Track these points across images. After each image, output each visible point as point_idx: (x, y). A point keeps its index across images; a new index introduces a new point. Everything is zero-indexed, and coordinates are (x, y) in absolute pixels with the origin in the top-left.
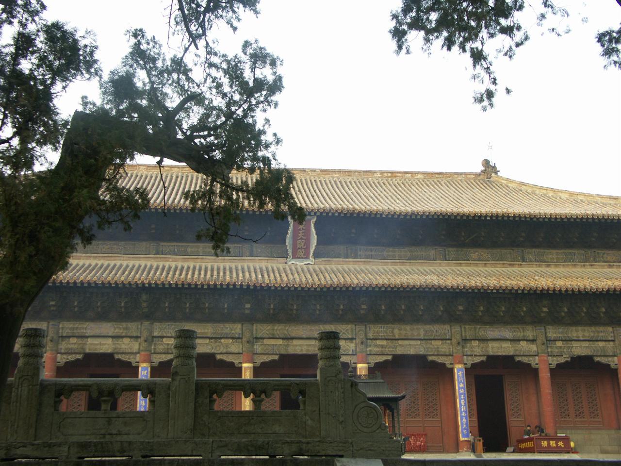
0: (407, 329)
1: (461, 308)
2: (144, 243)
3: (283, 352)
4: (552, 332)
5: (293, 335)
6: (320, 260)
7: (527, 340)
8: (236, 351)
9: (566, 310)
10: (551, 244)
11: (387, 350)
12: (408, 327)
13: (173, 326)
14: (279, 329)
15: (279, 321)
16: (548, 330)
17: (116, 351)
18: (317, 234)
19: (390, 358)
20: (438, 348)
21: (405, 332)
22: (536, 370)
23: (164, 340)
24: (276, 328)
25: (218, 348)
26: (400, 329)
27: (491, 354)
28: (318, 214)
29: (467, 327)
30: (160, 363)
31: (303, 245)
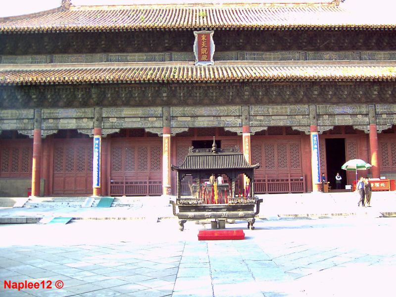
0: (278, 108)
1: (316, 93)
2: (99, 55)
3: (191, 126)
4: (380, 108)
6: (218, 62)
8: (159, 126)
9: (390, 93)
10: (380, 47)
12: (279, 107)
13: (115, 110)
14: (188, 110)
15: (188, 105)
16: (377, 107)
17: (78, 128)
18: (215, 44)
20: (300, 121)
21: (276, 111)
22: (368, 135)
23: (110, 119)
24: (186, 109)
25: (146, 124)
26: (273, 109)
27: (337, 124)
28: (215, 29)
29: (320, 106)
31: (205, 52)
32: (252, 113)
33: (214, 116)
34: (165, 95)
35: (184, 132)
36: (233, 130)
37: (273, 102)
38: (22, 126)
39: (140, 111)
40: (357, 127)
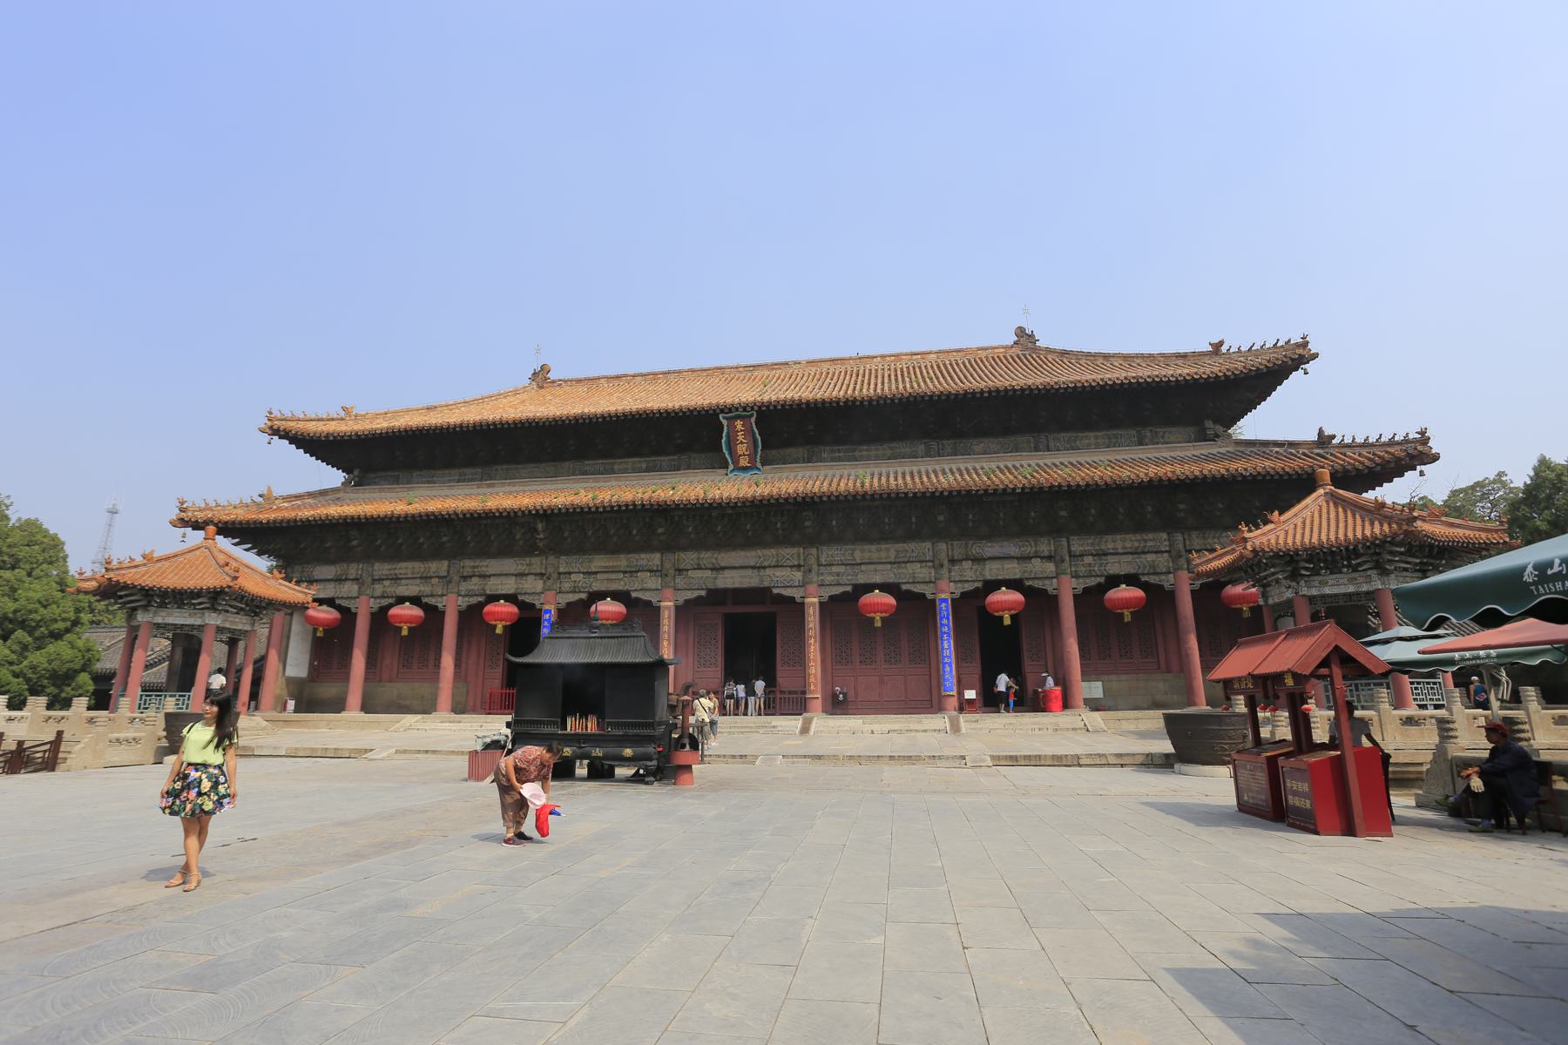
1: (941, 518)
3: (711, 586)
4: (1078, 545)
5: (723, 564)
11: (844, 579)
12: (874, 547)
14: (707, 557)
15: (707, 549)
19: (849, 589)
26: (862, 551)
30: (569, 604)
32: (823, 561)
33: (753, 568)
35: (700, 597)
36: (788, 592)
37: (863, 538)
39: (622, 561)
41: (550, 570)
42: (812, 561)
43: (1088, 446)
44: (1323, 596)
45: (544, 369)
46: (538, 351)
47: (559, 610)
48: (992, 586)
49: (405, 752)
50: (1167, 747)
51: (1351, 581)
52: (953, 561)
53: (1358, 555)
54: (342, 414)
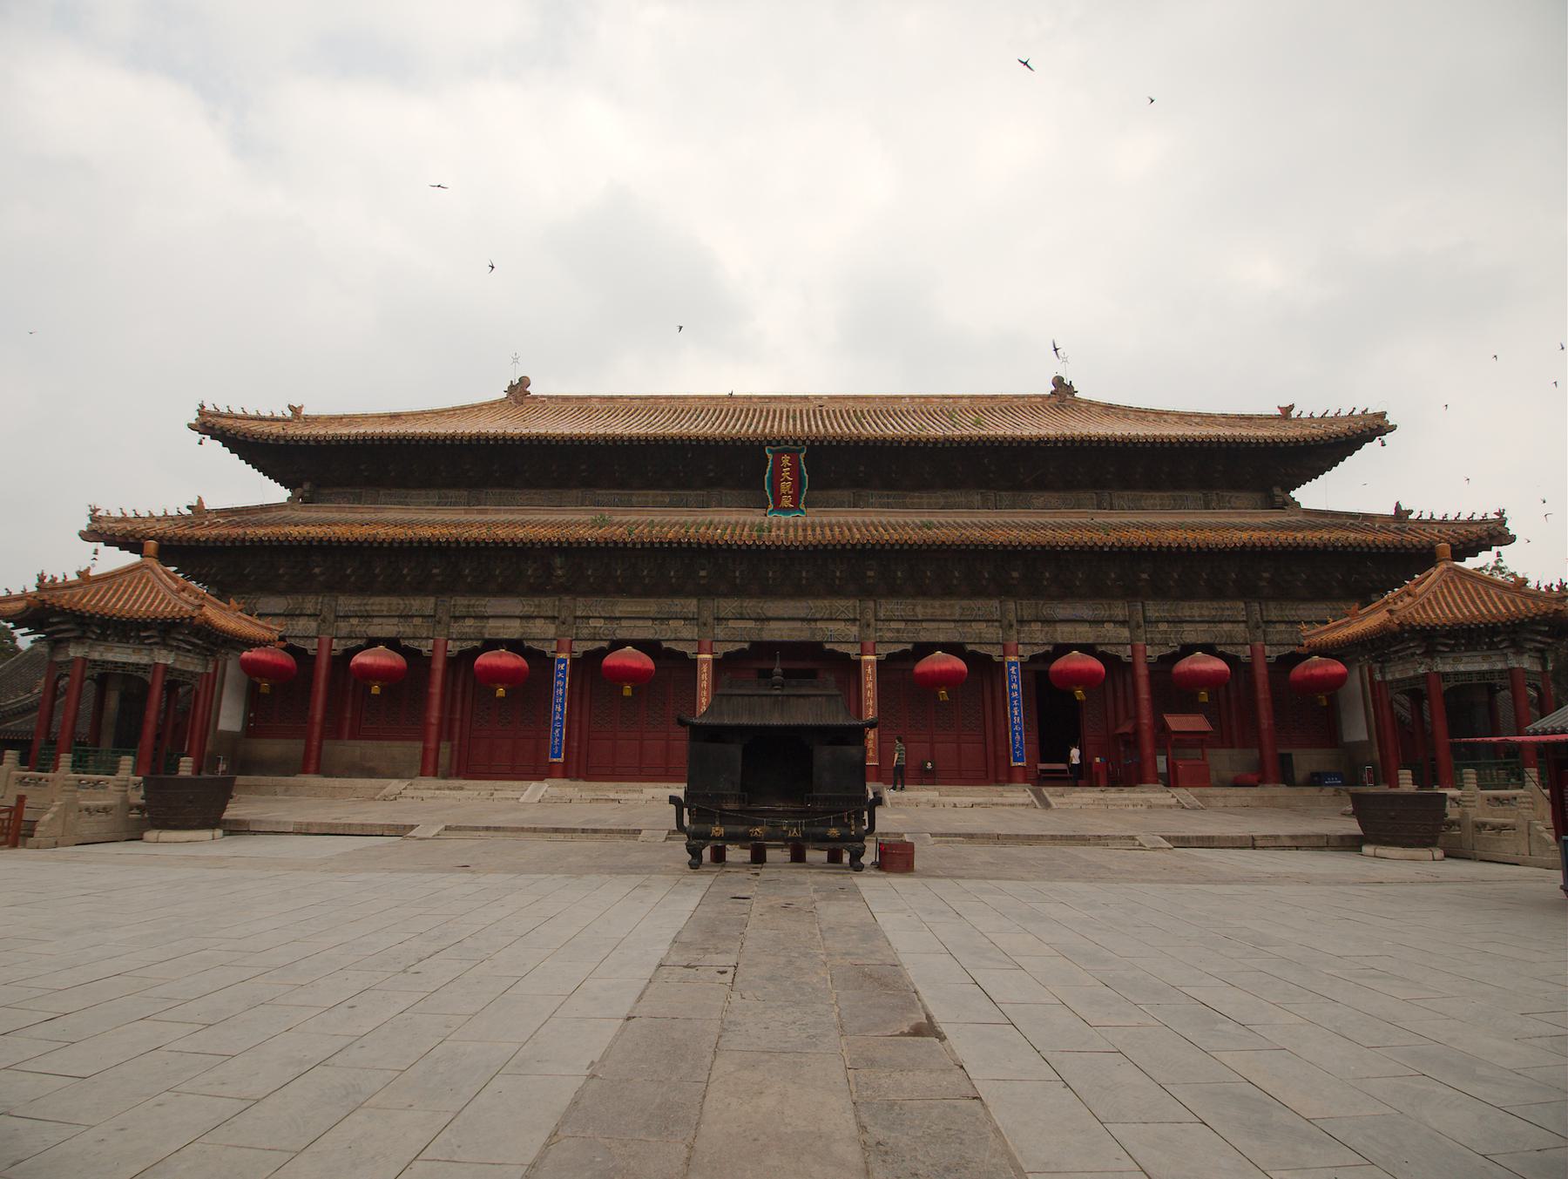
0: (935, 607)
1: (1015, 574)
3: (755, 638)
4: (1154, 610)
5: (770, 615)
7: (1115, 622)
11: (905, 636)
12: (937, 603)
14: (751, 605)
15: (751, 596)
19: (909, 647)
26: (925, 607)
32: (881, 615)
33: (803, 620)
34: (703, 573)
37: (922, 592)
38: (409, 631)
39: (651, 606)
40: (530, 644)
41: (564, 614)
42: (870, 616)
43: (1154, 507)
44: (1457, 674)
45: (524, 382)
46: (516, 360)
47: (572, 660)
48: (1062, 649)
49: (459, 829)
50: (1353, 827)
51: (1485, 658)
52: (1021, 622)
53: (1499, 634)
54: (289, 414)
